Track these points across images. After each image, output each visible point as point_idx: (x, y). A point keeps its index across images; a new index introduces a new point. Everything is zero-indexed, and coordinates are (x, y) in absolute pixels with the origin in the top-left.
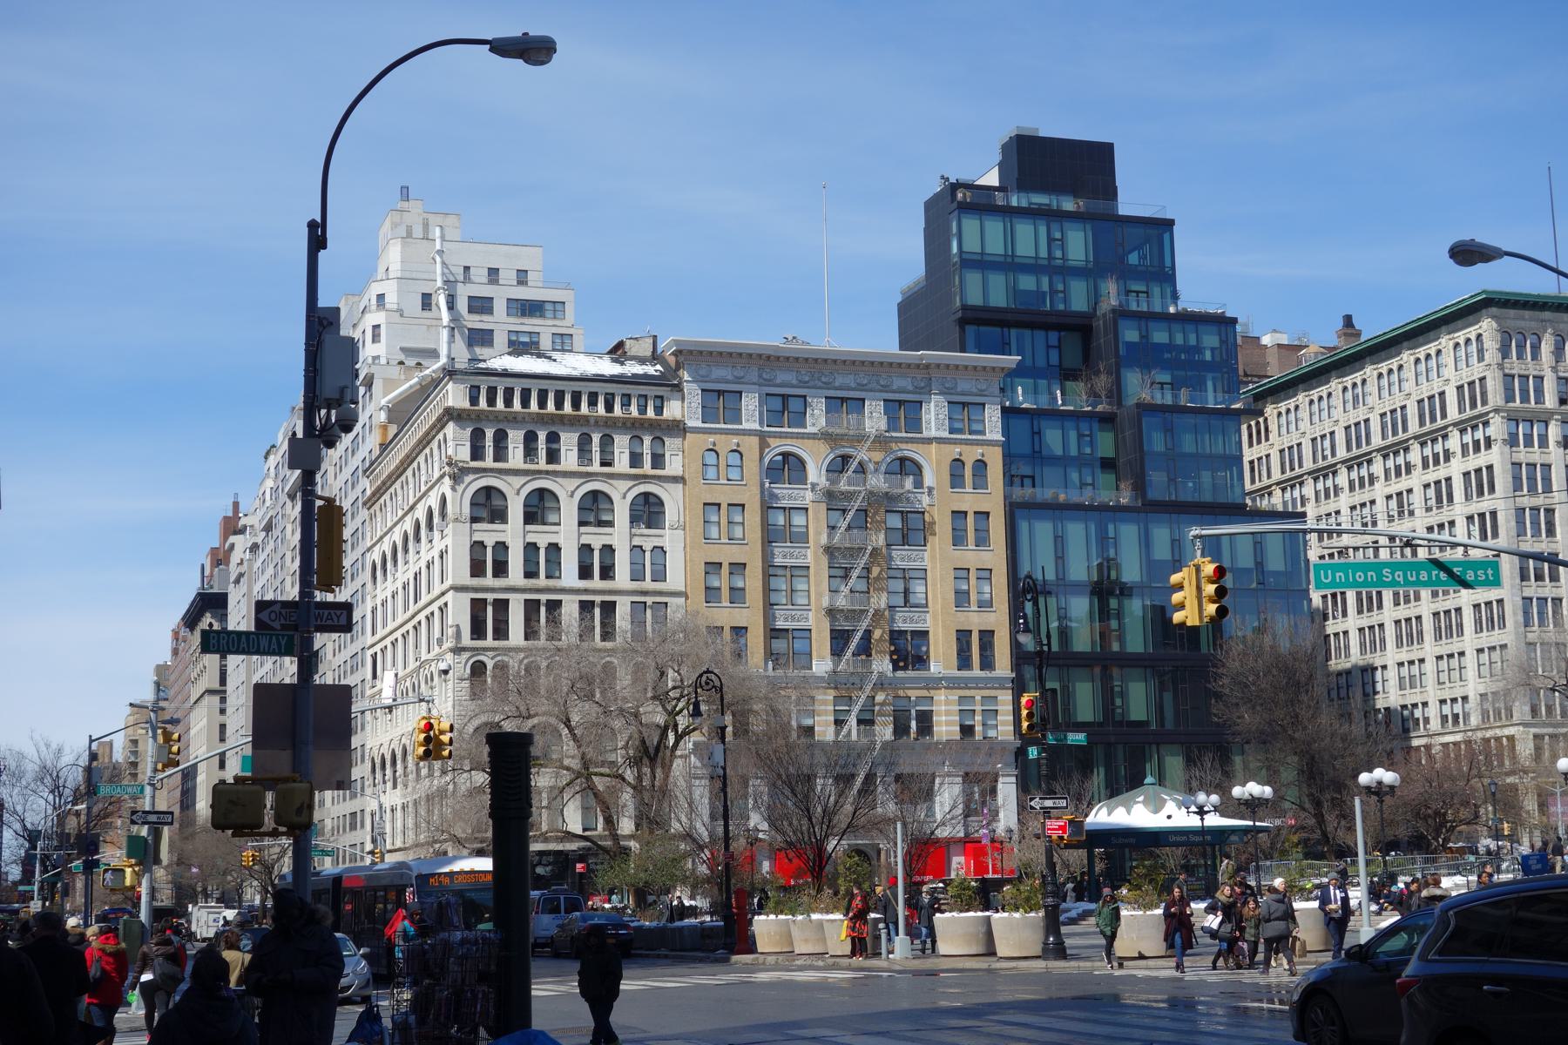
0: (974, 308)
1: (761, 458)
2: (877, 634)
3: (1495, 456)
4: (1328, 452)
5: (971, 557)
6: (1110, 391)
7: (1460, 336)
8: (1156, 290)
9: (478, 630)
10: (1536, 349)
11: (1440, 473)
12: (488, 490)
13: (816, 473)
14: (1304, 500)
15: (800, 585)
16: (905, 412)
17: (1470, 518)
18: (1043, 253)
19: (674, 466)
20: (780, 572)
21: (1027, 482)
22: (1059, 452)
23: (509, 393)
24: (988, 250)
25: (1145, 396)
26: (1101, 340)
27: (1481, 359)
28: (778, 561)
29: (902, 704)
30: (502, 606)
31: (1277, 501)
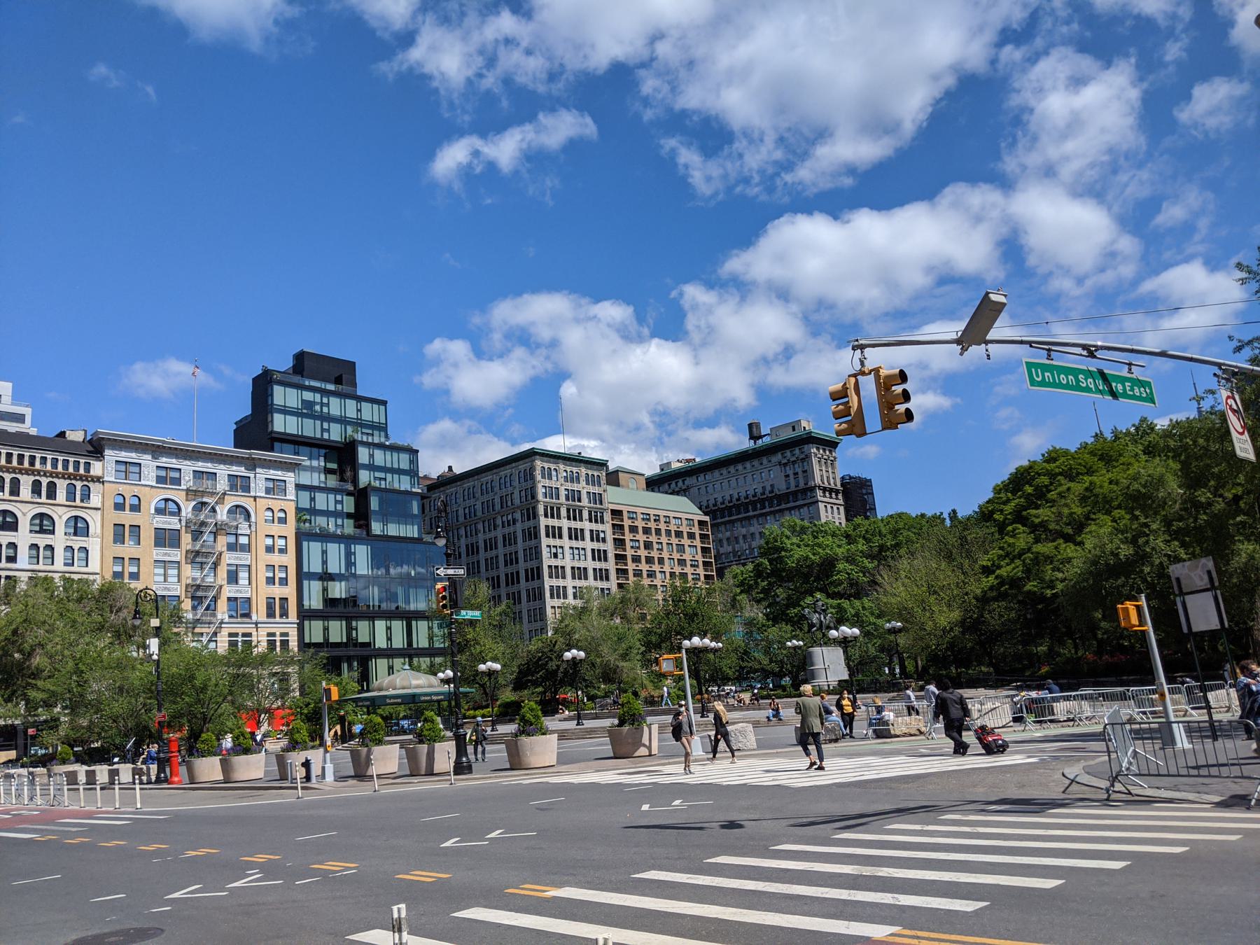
5: (276, 559)
19: (95, 500)
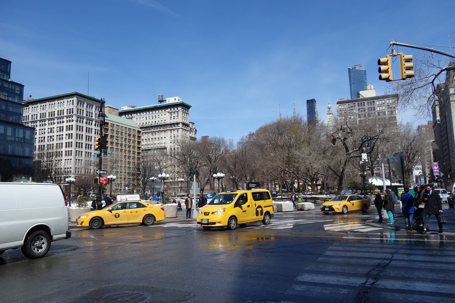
3: (74, 123)
4: (35, 118)
7: (69, 100)
8: (5, 76)
10: (83, 105)
11: (61, 125)
14: (36, 126)
17: (67, 135)
27: (73, 104)
31: (30, 125)
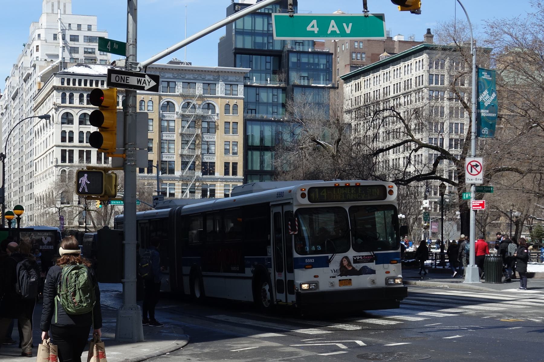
0: (239, 49)
1: (159, 103)
2: (197, 163)
5: (231, 137)
6: (285, 79)
9: (63, 160)
12: (67, 114)
13: (178, 108)
15: (172, 146)
16: (210, 86)
18: (266, 29)
20: (165, 142)
21: (253, 111)
22: (265, 101)
23: (74, 81)
24: (245, 28)
25: (297, 82)
26: (284, 60)
28: (164, 138)
29: (205, 187)
30: (71, 152)
